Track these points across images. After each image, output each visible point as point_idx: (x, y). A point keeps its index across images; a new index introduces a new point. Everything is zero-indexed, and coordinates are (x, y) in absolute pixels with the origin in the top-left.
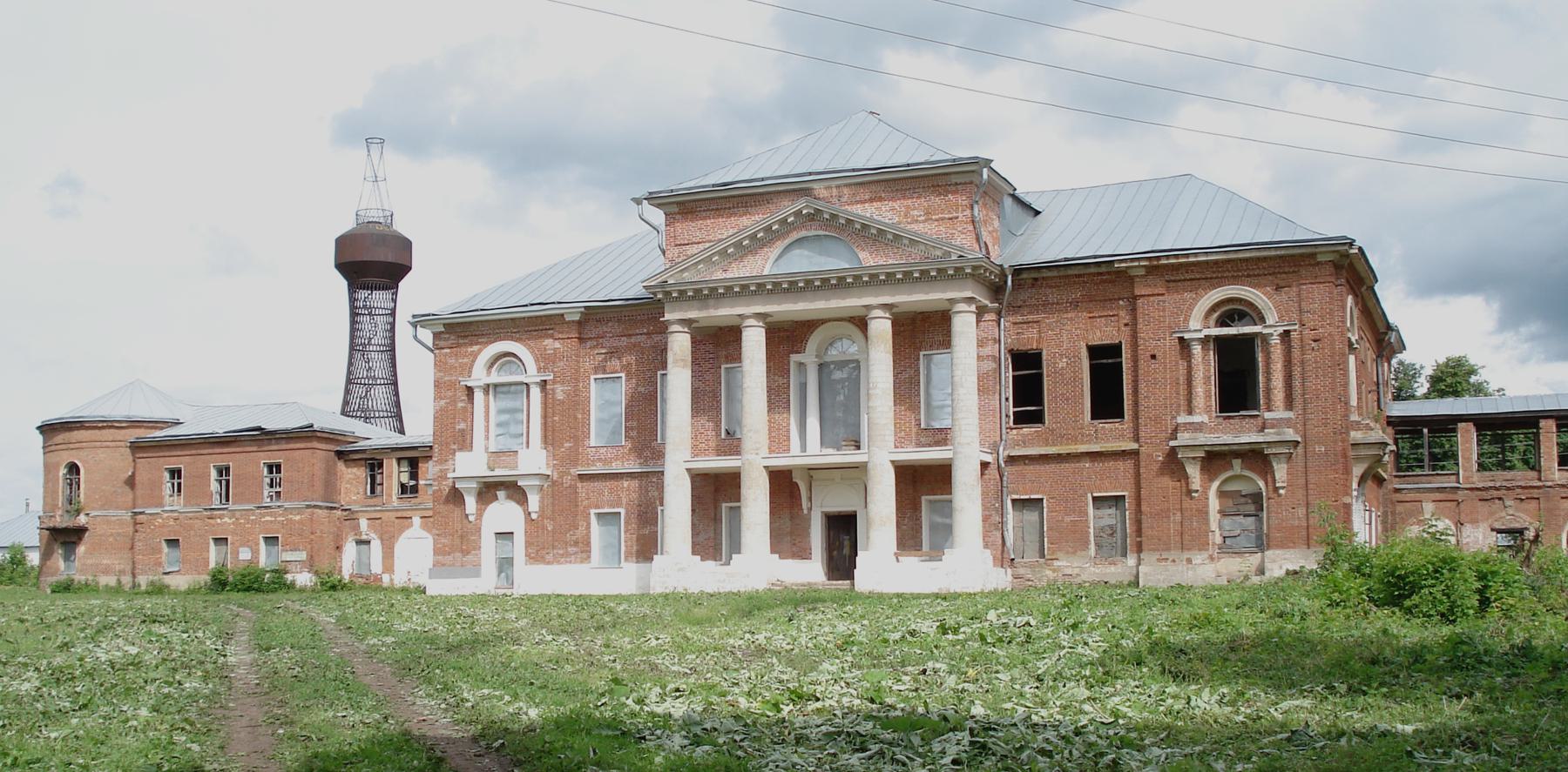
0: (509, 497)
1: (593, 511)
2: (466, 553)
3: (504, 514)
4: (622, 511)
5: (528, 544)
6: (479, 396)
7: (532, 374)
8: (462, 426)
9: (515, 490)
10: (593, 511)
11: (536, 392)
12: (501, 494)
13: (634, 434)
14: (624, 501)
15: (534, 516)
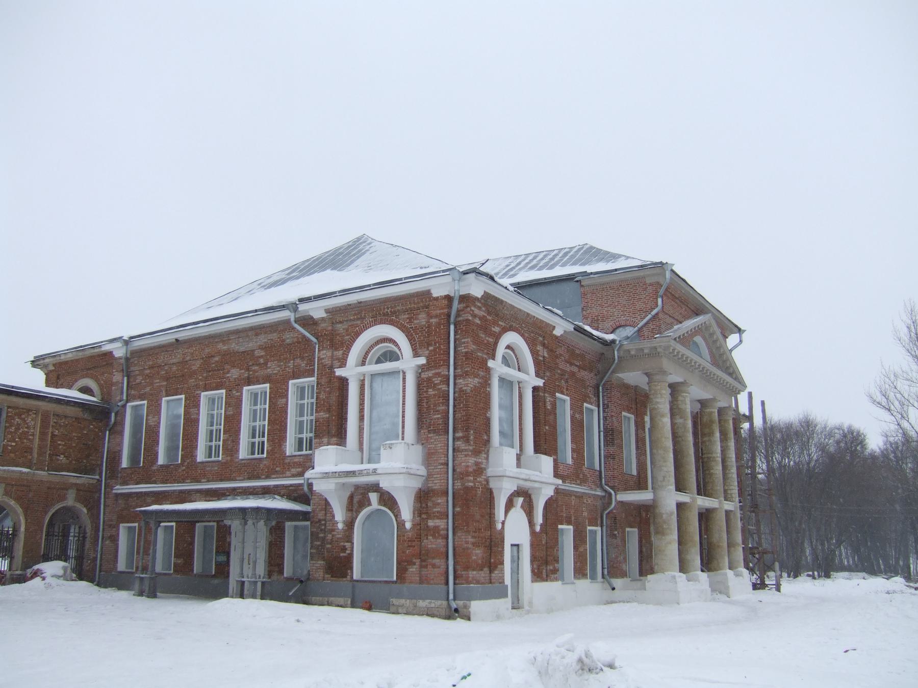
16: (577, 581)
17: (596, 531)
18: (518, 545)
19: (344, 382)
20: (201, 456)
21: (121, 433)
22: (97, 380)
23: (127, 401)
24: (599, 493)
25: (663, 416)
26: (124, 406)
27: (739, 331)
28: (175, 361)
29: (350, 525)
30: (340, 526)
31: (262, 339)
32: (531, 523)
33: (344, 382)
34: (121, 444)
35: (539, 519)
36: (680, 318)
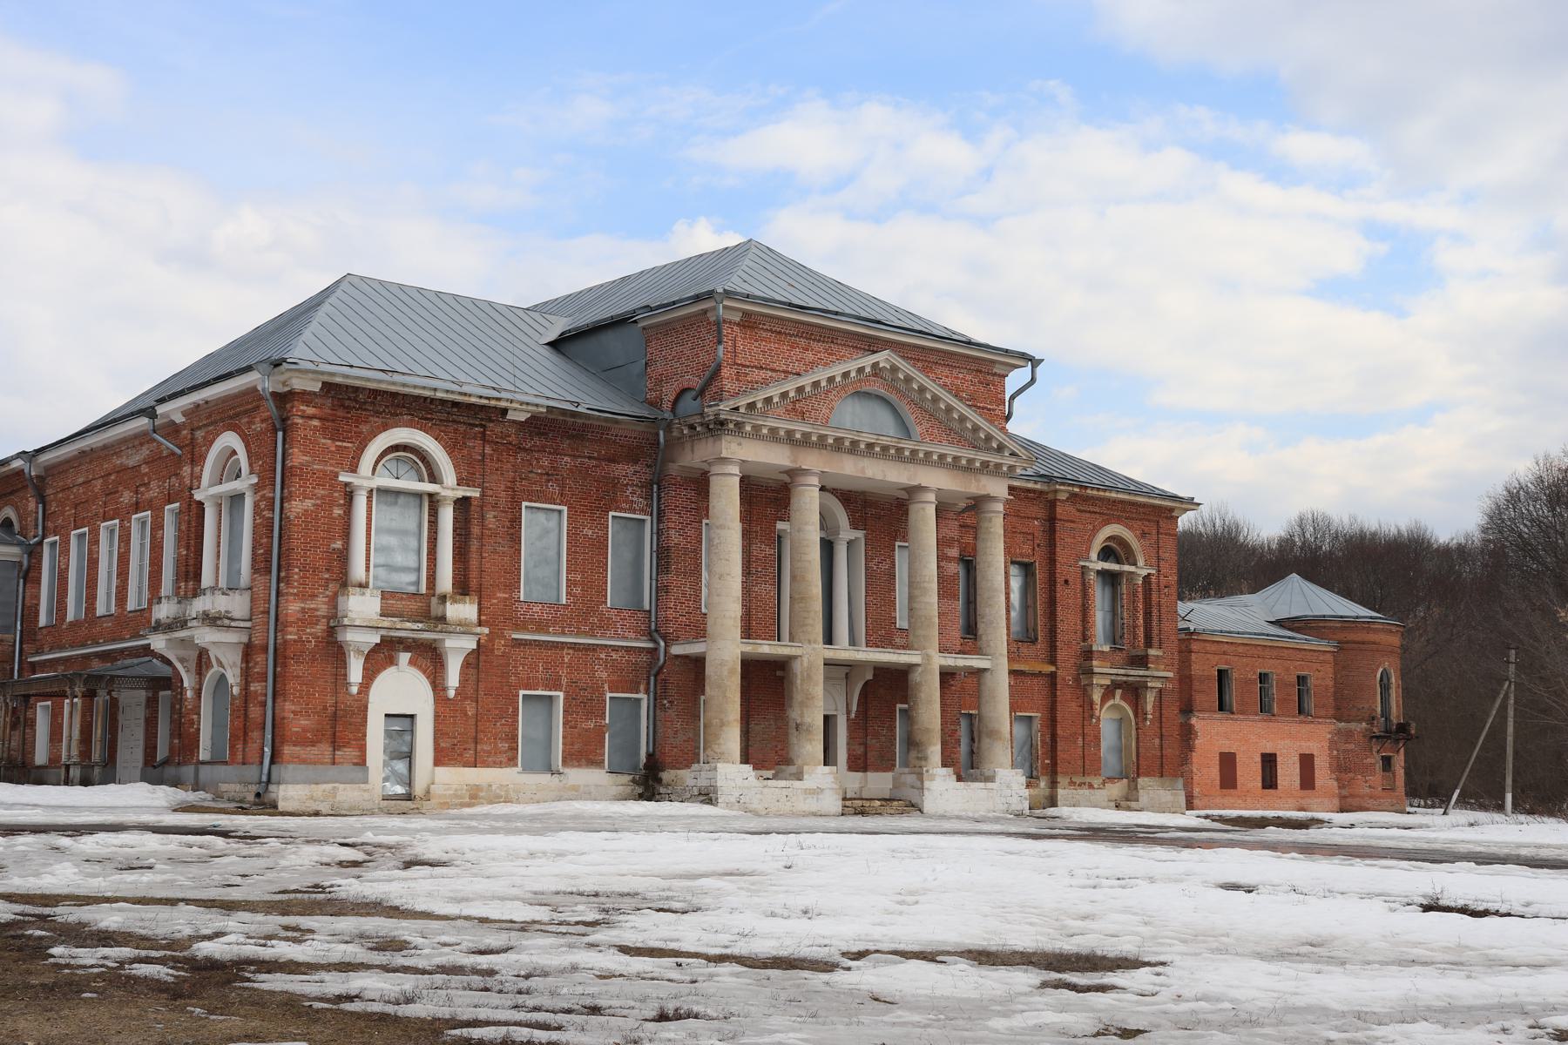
0: (412, 662)
1: (522, 692)
2: (336, 744)
3: (401, 690)
4: (561, 694)
5: (438, 734)
6: (360, 503)
7: (450, 487)
8: (338, 545)
9: (430, 658)
10: (522, 692)
11: (447, 516)
12: (404, 657)
13: (578, 590)
14: (564, 681)
15: (451, 694)
16: (567, 770)
17: (638, 701)
18: (412, 716)
19: (200, 504)
20: (100, 610)
21: (38, 581)
22: (17, 509)
23: (44, 537)
24: (650, 645)
25: (721, 527)
26: (40, 543)
27: (1035, 362)
28: (81, 480)
29: (198, 693)
30: (189, 694)
31: (145, 452)
32: (438, 686)
33: (200, 504)
34: (38, 597)
35: (453, 679)
36: (797, 367)
